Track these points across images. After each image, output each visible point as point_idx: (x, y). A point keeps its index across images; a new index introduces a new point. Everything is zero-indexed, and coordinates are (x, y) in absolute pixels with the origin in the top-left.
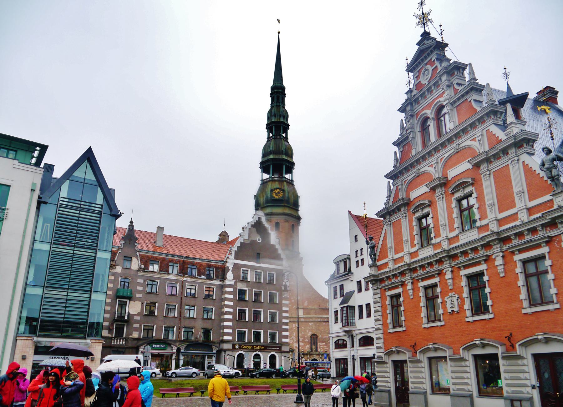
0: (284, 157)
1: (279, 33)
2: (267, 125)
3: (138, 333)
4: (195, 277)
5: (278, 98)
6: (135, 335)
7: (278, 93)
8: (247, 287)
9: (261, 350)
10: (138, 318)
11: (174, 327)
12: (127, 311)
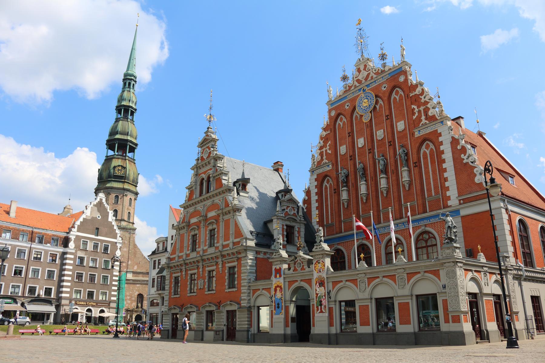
0: (129, 138)
5: (130, 84)
8: (85, 255)
9: (93, 306)
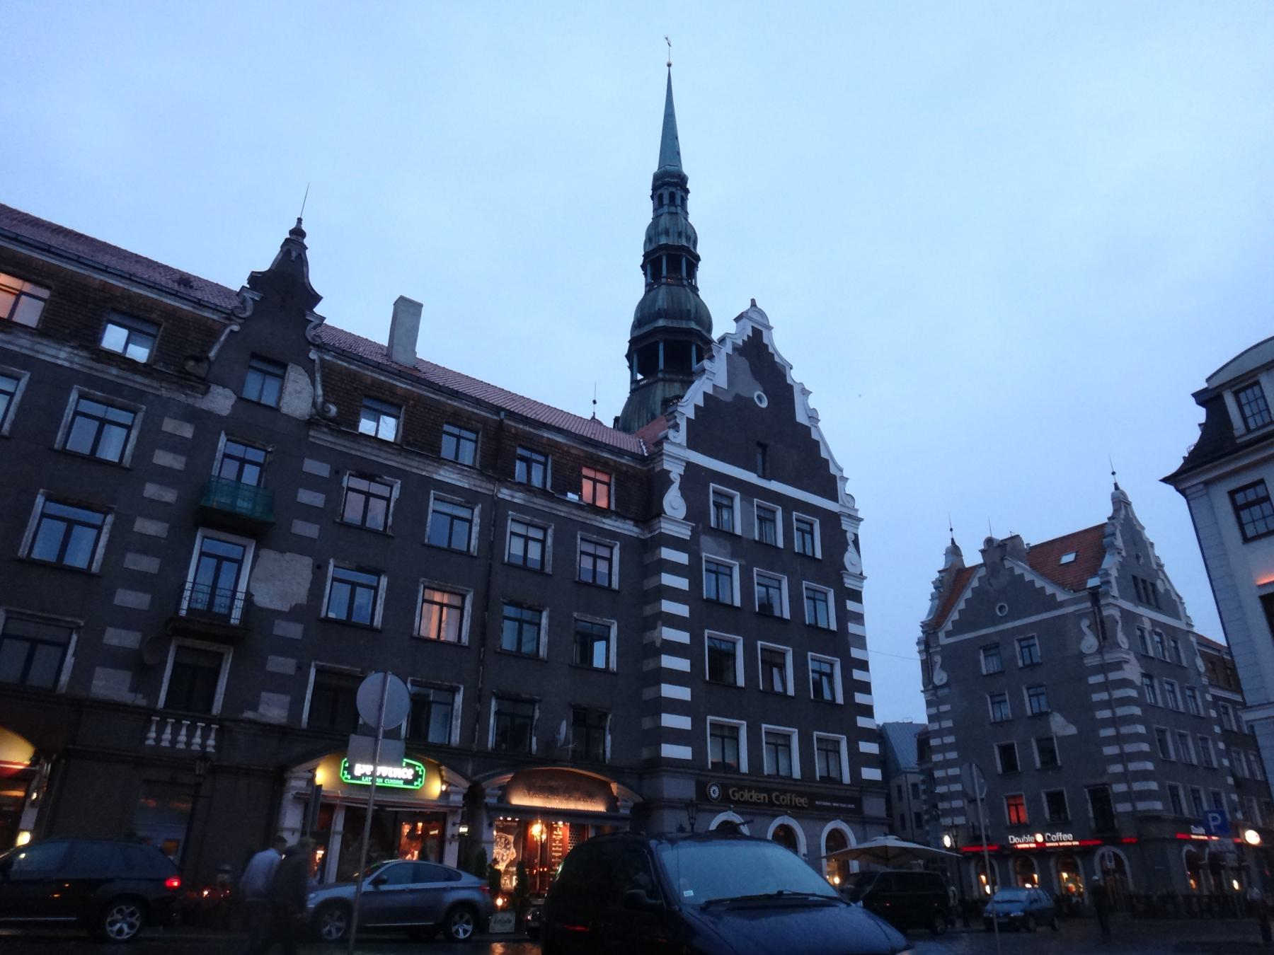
0: (693, 325)
1: (669, 65)
2: (646, 256)
3: (286, 699)
4: (543, 492)
5: (672, 196)
6: (273, 710)
7: (670, 188)
8: (733, 557)
10: (294, 630)
11: (454, 690)
12: (242, 587)
